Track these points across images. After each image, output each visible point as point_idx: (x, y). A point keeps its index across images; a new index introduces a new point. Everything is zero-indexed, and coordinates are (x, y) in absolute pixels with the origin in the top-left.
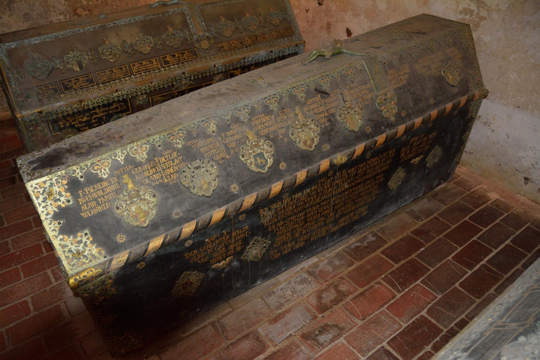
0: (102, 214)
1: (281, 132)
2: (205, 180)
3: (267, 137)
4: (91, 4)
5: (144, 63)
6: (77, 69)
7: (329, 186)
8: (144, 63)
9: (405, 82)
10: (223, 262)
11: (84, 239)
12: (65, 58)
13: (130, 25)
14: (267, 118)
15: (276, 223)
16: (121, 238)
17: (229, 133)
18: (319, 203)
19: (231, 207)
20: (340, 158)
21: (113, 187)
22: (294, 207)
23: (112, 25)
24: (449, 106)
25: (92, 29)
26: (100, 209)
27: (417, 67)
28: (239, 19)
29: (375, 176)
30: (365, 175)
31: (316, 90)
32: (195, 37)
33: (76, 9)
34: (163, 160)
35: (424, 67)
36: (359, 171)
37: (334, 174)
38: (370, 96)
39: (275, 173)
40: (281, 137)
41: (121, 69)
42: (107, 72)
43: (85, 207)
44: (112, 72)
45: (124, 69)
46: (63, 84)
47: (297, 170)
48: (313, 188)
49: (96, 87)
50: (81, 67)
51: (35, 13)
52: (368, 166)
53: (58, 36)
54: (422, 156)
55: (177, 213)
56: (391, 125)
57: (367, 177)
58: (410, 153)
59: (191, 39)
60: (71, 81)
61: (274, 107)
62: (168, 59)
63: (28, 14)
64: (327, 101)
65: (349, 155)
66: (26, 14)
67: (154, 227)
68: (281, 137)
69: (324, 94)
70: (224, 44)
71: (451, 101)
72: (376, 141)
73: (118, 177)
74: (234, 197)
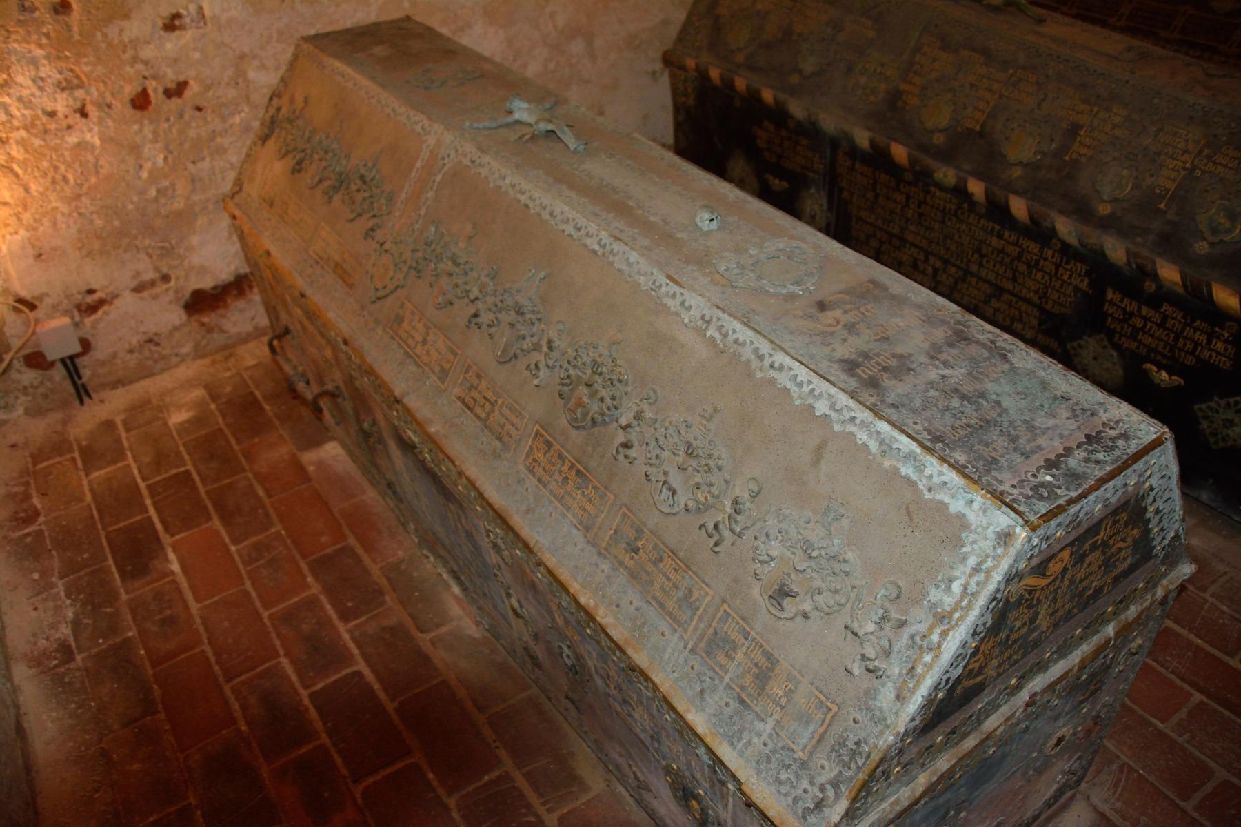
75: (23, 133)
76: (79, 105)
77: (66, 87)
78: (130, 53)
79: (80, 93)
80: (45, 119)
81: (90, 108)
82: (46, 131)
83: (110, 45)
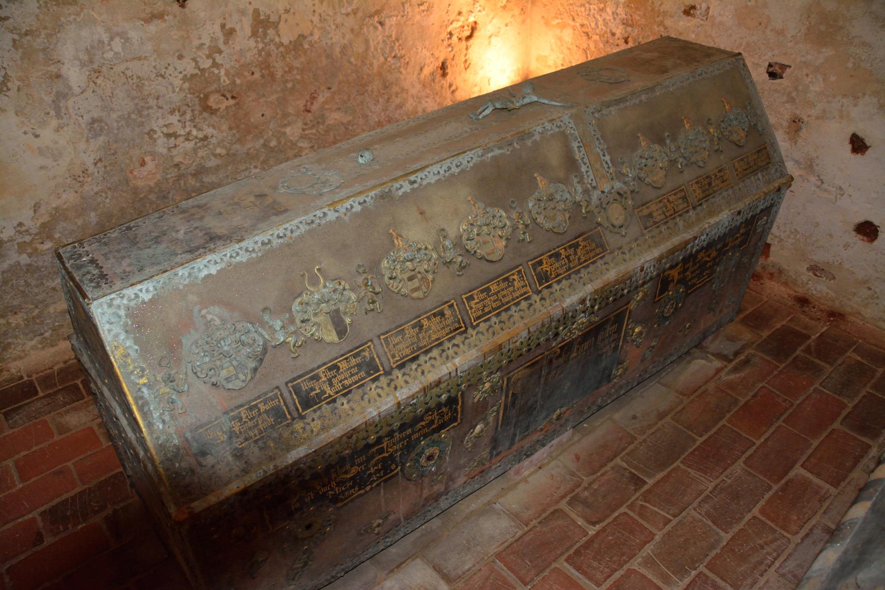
4: (238, 81)
5: (494, 288)
6: (332, 336)
12: (296, 307)
13: (449, 181)
23: (407, 187)
25: (358, 208)
28: (674, 138)
33: (207, 97)
41: (442, 314)
42: (410, 332)
44: (421, 327)
45: (448, 312)
46: (297, 390)
49: (384, 380)
50: (342, 333)
51: (114, 116)
53: (270, 241)
59: (588, 203)
60: (316, 378)
63: (100, 120)
66: (94, 121)
70: (653, 207)
75: (597, 37)
76: (626, 35)
77: (625, 23)
78: (661, 18)
79: (629, 29)
80: (609, 35)
81: (630, 39)
82: (607, 42)
83: (653, 10)
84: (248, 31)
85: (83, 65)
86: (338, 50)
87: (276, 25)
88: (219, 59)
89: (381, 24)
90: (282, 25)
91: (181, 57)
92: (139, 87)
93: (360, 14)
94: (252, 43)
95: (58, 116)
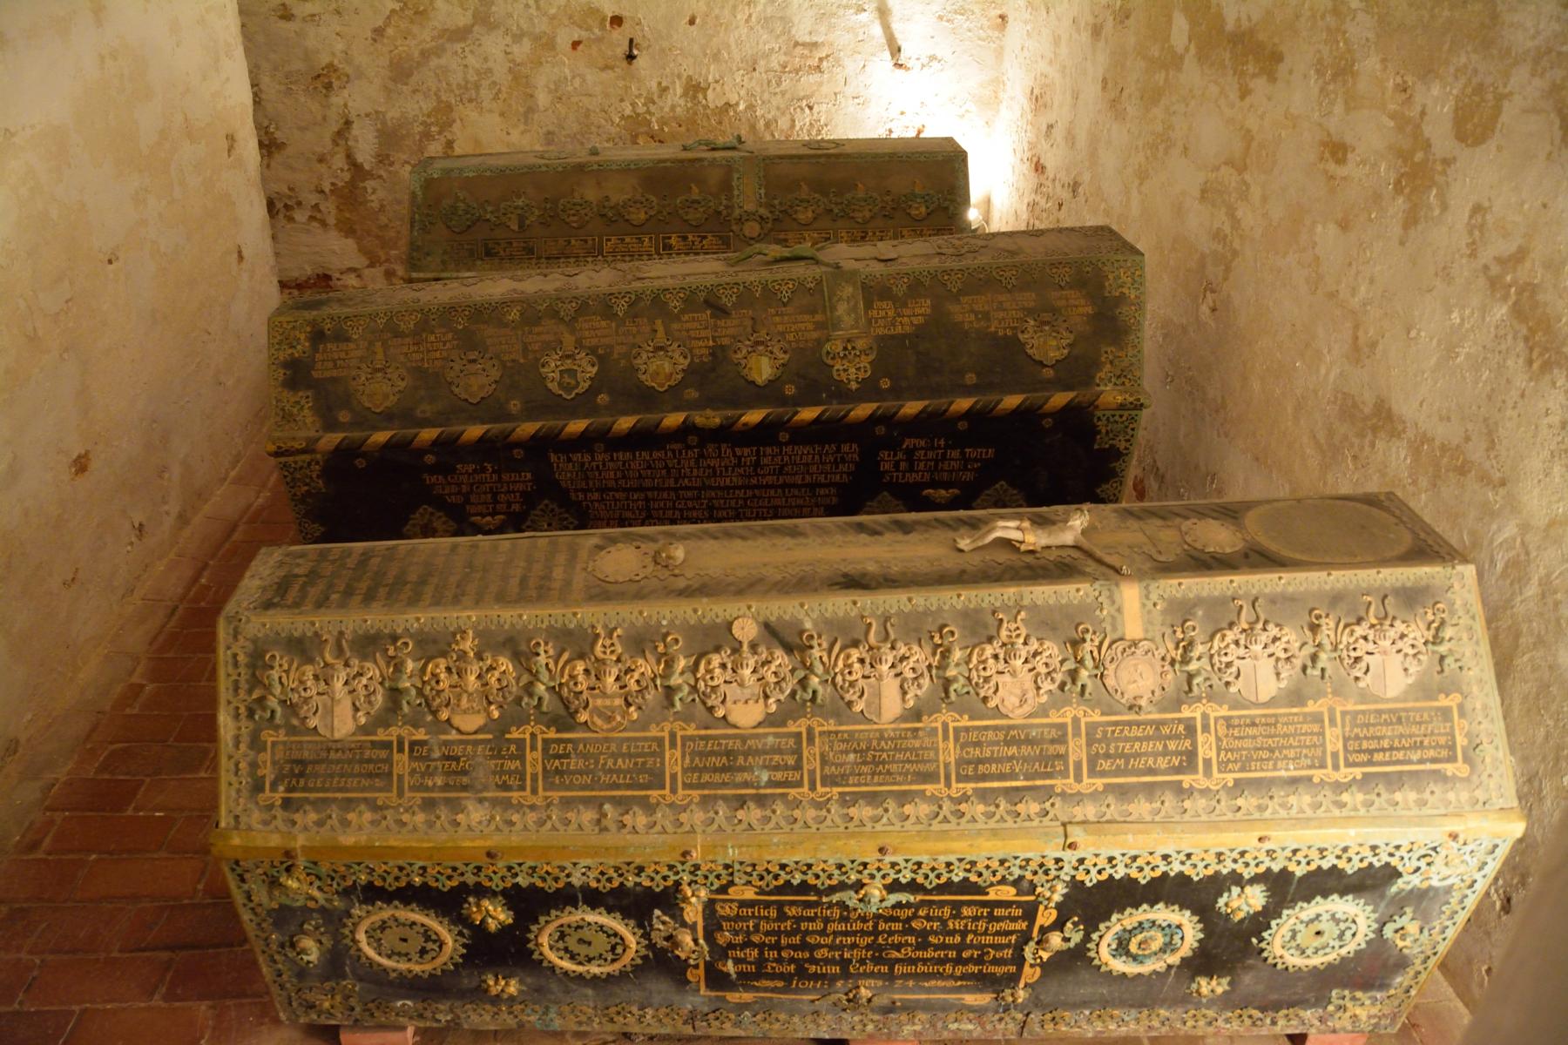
0: (334, 380)
1: (618, 350)
2: (478, 381)
3: (593, 351)
5: (628, 240)
6: (515, 228)
7: (692, 463)
8: (628, 240)
9: (908, 329)
10: (489, 518)
11: (303, 402)
14: (604, 323)
15: (582, 490)
16: (344, 416)
17: (536, 330)
18: (676, 490)
19: (496, 427)
20: (711, 418)
21: (359, 353)
22: (619, 474)
24: (1012, 401)
26: (335, 373)
27: (953, 308)
29: (813, 486)
30: (781, 472)
31: (706, 302)
32: (737, 212)
33: (636, 136)
34: (432, 338)
35: (972, 311)
36: (765, 461)
37: (701, 445)
38: (815, 335)
39: (583, 404)
40: (616, 356)
43: (318, 366)
47: (626, 413)
48: (656, 454)
52: (786, 459)
54: (956, 491)
55: (425, 409)
56: (842, 394)
57: (789, 480)
58: (911, 470)
61: (621, 308)
62: (673, 241)
64: (721, 323)
65: (727, 418)
66: (549, 133)
67: (388, 417)
68: (616, 356)
69: (720, 311)
71: (1022, 392)
72: (796, 413)
73: (371, 343)
74: (508, 417)
84: (679, 91)
85: (550, 92)
86: (762, 122)
87: (705, 90)
88: (652, 108)
89: (811, 108)
90: (710, 92)
91: (622, 100)
92: (587, 116)
93: (788, 96)
94: (682, 102)
95: (526, 123)
